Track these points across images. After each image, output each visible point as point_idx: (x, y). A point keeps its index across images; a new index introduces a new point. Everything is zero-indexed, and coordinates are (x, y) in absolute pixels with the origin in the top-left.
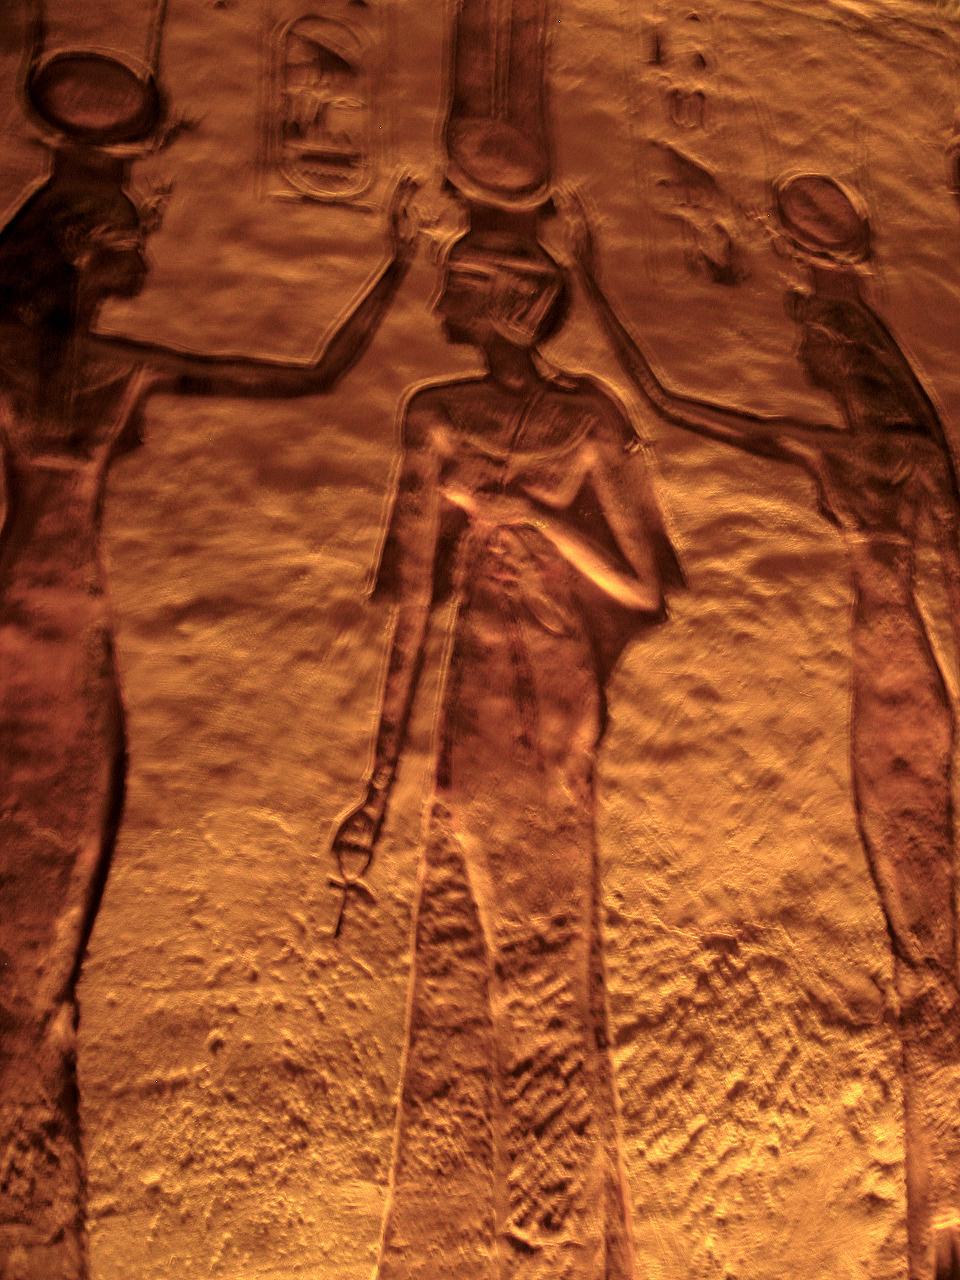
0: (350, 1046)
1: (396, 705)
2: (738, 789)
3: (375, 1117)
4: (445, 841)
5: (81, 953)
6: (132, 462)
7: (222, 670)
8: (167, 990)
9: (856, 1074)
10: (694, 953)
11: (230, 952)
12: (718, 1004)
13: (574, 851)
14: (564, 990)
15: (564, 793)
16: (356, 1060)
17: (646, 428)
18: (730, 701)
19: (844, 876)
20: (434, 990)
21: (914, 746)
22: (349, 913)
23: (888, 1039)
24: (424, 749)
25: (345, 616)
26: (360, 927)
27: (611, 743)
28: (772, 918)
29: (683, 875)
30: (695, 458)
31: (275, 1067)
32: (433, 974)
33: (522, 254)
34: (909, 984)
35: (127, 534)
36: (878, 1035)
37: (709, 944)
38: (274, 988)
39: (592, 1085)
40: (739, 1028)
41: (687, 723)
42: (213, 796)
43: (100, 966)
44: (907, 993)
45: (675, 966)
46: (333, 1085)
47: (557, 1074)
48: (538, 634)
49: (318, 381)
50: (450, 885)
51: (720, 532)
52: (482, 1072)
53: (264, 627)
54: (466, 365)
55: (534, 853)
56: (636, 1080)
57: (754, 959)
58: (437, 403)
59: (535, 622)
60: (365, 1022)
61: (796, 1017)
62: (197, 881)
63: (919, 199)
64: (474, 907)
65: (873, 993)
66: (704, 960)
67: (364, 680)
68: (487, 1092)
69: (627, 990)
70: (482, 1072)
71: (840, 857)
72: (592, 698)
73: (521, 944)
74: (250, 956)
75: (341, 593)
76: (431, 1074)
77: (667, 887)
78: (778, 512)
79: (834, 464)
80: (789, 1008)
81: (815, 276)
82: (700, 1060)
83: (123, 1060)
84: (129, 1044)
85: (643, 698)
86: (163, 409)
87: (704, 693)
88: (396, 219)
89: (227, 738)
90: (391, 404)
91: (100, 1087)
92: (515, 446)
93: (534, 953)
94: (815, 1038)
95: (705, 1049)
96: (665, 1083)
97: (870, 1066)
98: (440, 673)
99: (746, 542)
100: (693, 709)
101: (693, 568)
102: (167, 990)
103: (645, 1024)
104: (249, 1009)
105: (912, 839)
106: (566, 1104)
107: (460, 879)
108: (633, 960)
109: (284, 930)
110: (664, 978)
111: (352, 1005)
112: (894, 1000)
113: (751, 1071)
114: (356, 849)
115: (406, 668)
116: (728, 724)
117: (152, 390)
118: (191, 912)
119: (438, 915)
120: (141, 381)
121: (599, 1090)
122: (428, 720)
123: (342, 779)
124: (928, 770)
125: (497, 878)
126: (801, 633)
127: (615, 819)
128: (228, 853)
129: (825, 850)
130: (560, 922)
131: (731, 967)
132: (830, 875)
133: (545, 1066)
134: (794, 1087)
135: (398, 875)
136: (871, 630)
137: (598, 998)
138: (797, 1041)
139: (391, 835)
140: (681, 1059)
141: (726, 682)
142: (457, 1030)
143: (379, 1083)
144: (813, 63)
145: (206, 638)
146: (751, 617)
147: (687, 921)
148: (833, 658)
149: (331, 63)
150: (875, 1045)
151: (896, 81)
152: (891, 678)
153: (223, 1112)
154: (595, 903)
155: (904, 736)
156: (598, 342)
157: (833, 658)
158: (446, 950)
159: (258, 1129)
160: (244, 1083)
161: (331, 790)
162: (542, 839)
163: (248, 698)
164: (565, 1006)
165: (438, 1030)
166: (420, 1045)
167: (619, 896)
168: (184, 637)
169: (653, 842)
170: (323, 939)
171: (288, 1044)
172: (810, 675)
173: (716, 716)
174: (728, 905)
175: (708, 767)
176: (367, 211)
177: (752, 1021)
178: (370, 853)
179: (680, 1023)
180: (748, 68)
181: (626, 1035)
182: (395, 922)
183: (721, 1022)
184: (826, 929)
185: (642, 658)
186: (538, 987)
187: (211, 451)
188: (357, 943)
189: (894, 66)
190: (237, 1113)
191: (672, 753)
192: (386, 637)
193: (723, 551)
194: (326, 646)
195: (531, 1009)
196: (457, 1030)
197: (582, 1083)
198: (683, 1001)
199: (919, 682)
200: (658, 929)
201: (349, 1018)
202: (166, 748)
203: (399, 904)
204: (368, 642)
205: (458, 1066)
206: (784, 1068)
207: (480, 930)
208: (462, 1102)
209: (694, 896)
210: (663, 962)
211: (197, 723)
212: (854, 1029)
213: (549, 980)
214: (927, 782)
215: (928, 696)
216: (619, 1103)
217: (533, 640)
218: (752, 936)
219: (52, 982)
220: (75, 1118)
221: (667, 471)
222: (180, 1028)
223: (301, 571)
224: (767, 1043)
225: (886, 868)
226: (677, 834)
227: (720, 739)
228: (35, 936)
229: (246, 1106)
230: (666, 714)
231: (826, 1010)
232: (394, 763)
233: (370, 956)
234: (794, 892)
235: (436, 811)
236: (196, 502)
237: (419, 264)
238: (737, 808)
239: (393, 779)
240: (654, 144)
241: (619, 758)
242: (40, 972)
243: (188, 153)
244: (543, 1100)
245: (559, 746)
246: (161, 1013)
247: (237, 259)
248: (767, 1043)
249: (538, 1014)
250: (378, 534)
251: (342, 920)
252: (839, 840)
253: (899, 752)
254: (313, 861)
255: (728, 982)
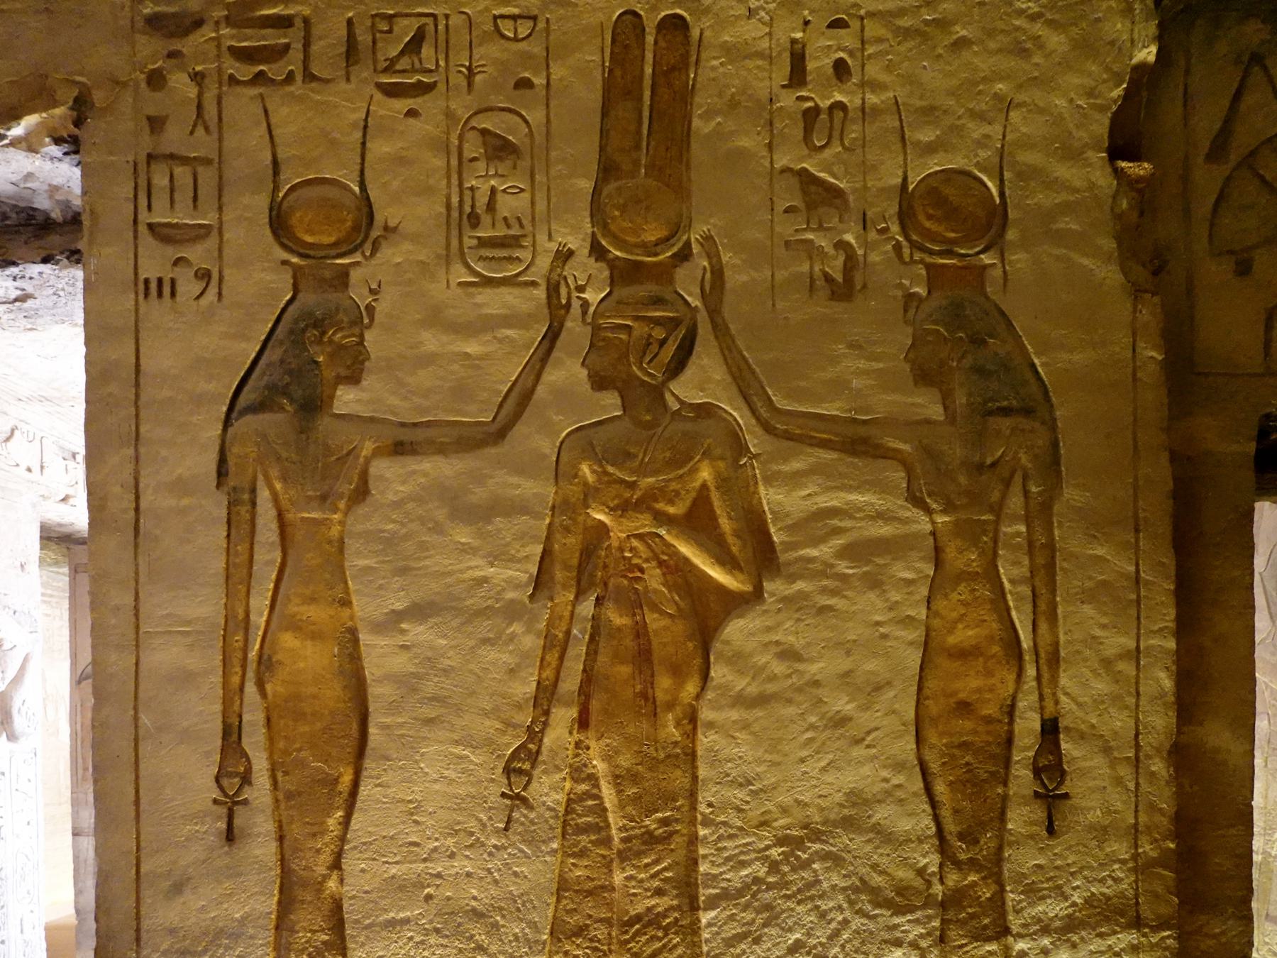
0: (515, 902)
1: (548, 673)
2: (812, 727)
3: (530, 948)
4: (585, 765)
5: (343, 839)
6: (361, 510)
7: (430, 654)
8: (397, 863)
9: (898, 943)
10: (768, 848)
11: (437, 839)
12: (786, 885)
13: (678, 773)
14: (665, 869)
15: (671, 730)
16: (518, 910)
17: (755, 441)
18: (812, 660)
19: (900, 794)
20: (573, 864)
21: (979, 690)
22: (515, 815)
23: (930, 918)
24: (568, 704)
25: (512, 612)
26: (522, 824)
27: (710, 695)
28: (835, 824)
29: (761, 790)
30: (796, 465)
31: (467, 912)
32: (574, 855)
33: (658, 301)
34: (953, 878)
35: (362, 562)
36: (919, 914)
37: (781, 841)
38: (466, 863)
39: (683, 933)
40: (799, 903)
41: (773, 678)
42: (425, 738)
43: (355, 848)
44: (950, 884)
45: (753, 855)
46: (503, 926)
47: (659, 928)
48: (656, 616)
49: (499, 433)
50: (587, 795)
51: (817, 524)
52: (607, 922)
53: (455, 623)
54: (604, 409)
55: (648, 775)
56: (718, 933)
57: (816, 852)
58: (585, 441)
59: (655, 608)
60: (525, 886)
61: (848, 896)
62: (416, 792)
63: (1063, 171)
64: (605, 810)
65: (918, 883)
66: (775, 852)
67: (525, 655)
68: (609, 934)
69: (715, 871)
70: (607, 922)
71: (898, 779)
72: (698, 661)
73: (636, 837)
74: (450, 842)
75: (510, 595)
76: (572, 920)
77: (748, 799)
78: (870, 503)
79: (929, 452)
80: (844, 889)
81: (935, 276)
82: (765, 925)
83: (371, 905)
84: (374, 895)
85: (737, 660)
86: (384, 469)
87: (789, 655)
88: (553, 290)
89: (434, 699)
90: (547, 447)
91: (357, 921)
92: (643, 471)
93: (644, 843)
94: (861, 913)
95: (772, 915)
96: (740, 937)
97: (911, 936)
98: (578, 651)
99: (837, 531)
100: (779, 668)
101: (783, 557)
102: (397, 863)
103: (725, 895)
104: (450, 875)
105: (967, 764)
106: (664, 946)
107: (595, 791)
108: (718, 849)
109: (472, 825)
110: (743, 864)
111: (516, 874)
112: (938, 889)
113: (809, 935)
114: (520, 772)
115: (556, 645)
116: (807, 677)
117: (377, 453)
118: (412, 814)
119: (580, 816)
120: (368, 448)
121: (689, 938)
122: (571, 683)
123: (508, 724)
124: (990, 710)
125: (619, 792)
126: (880, 604)
127: (710, 750)
128: (435, 776)
129: (885, 774)
130: (665, 822)
131: (798, 858)
132: (888, 793)
133: (650, 920)
134: (843, 947)
135: (549, 790)
136: (946, 595)
137: (693, 875)
138: (847, 914)
139: (544, 762)
140: (754, 921)
141: (809, 644)
142: (590, 893)
143: (533, 925)
144: (961, 44)
145: (417, 632)
146: (834, 593)
147: (763, 824)
148: (908, 621)
149: (499, 149)
150: (917, 921)
151: (1056, 41)
152: (963, 635)
153: (433, 940)
154: (694, 808)
155: (969, 684)
156: (718, 373)
157: (908, 621)
158: (584, 840)
159: (454, 951)
160: (445, 922)
161: (504, 733)
162: (654, 764)
163: (446, 672)
164: (666, 880)
165: (577, 892)
166: (564, 902)
167: (710, 805)
168: (403, 632)
169: (738, 765)
170: (497, 831)
171: (475, 898)
172: (884, 637)
173: (801, 673)
174: (799, 814)
175: (791, 711)
176: (533, 284)
177: (812, 898)
178: (528, 774)
179: (753, 896)
180: (889, 68)
181: (712, 903)
182: (546, 821)
183: (788, 897)
184: (878, 833)
185: (737, 631)
186: (647, 865)
187: (418, 499)
188: (519, 834)
189: (1051, 23)
190: (442, 941)
191: (761, 700)
192: (542, 625)
193: (816, 542)
194: (499, 635)
195: (642, 881)
196: (590, 893)
197: (676, 933)
198: (757, 880)
199: (990, 638)
200: (741, 829)
201: (515, 883)
202: (393, 707)
203: (550, 809)
204: (528, 631)
205: (590, 916)
206: (836, 934)
207: (608, 826)
208: (591, 940)
209: (769, 806)
210: (742, 853)
211: (415, 690)
212: (899, 911)
213: (656, 862)
214: (988, 720)
215: (996, 649)
216: (705, 949)
217: (654, 621)
218: (817, 836)
219: (326, 858)
220: (342, 938)
221: (768, 481)
222: (405, 886)
223: (485, 580)
224: (823, 915)
225: (940, 788)
226: (759, 761)
227: (800, 690)
228: (315, 829)
229: (447, 936)
230: (758, 672)
231: (874, 892)
232: (547, 713)
233: (529, 843)
234: (854, 805)
235: (578, 745)
236: (407, 537)
237: (574, 326)
238: (811, 740)
239: (545, 724)
240: (786, 170)
241: (716, 707)
242: (318, 851)
243: (392, 254)
244: (648, 942)
245: (668, 697)
246: (393, 877)
247: (431, 341)
248: (823, 915)
249: (647, 885)
250: (539, 549)
251: (508, 822)
252: (899, 767)
253: (962, 696)
254: (493, 780)
255: (794, 870)
